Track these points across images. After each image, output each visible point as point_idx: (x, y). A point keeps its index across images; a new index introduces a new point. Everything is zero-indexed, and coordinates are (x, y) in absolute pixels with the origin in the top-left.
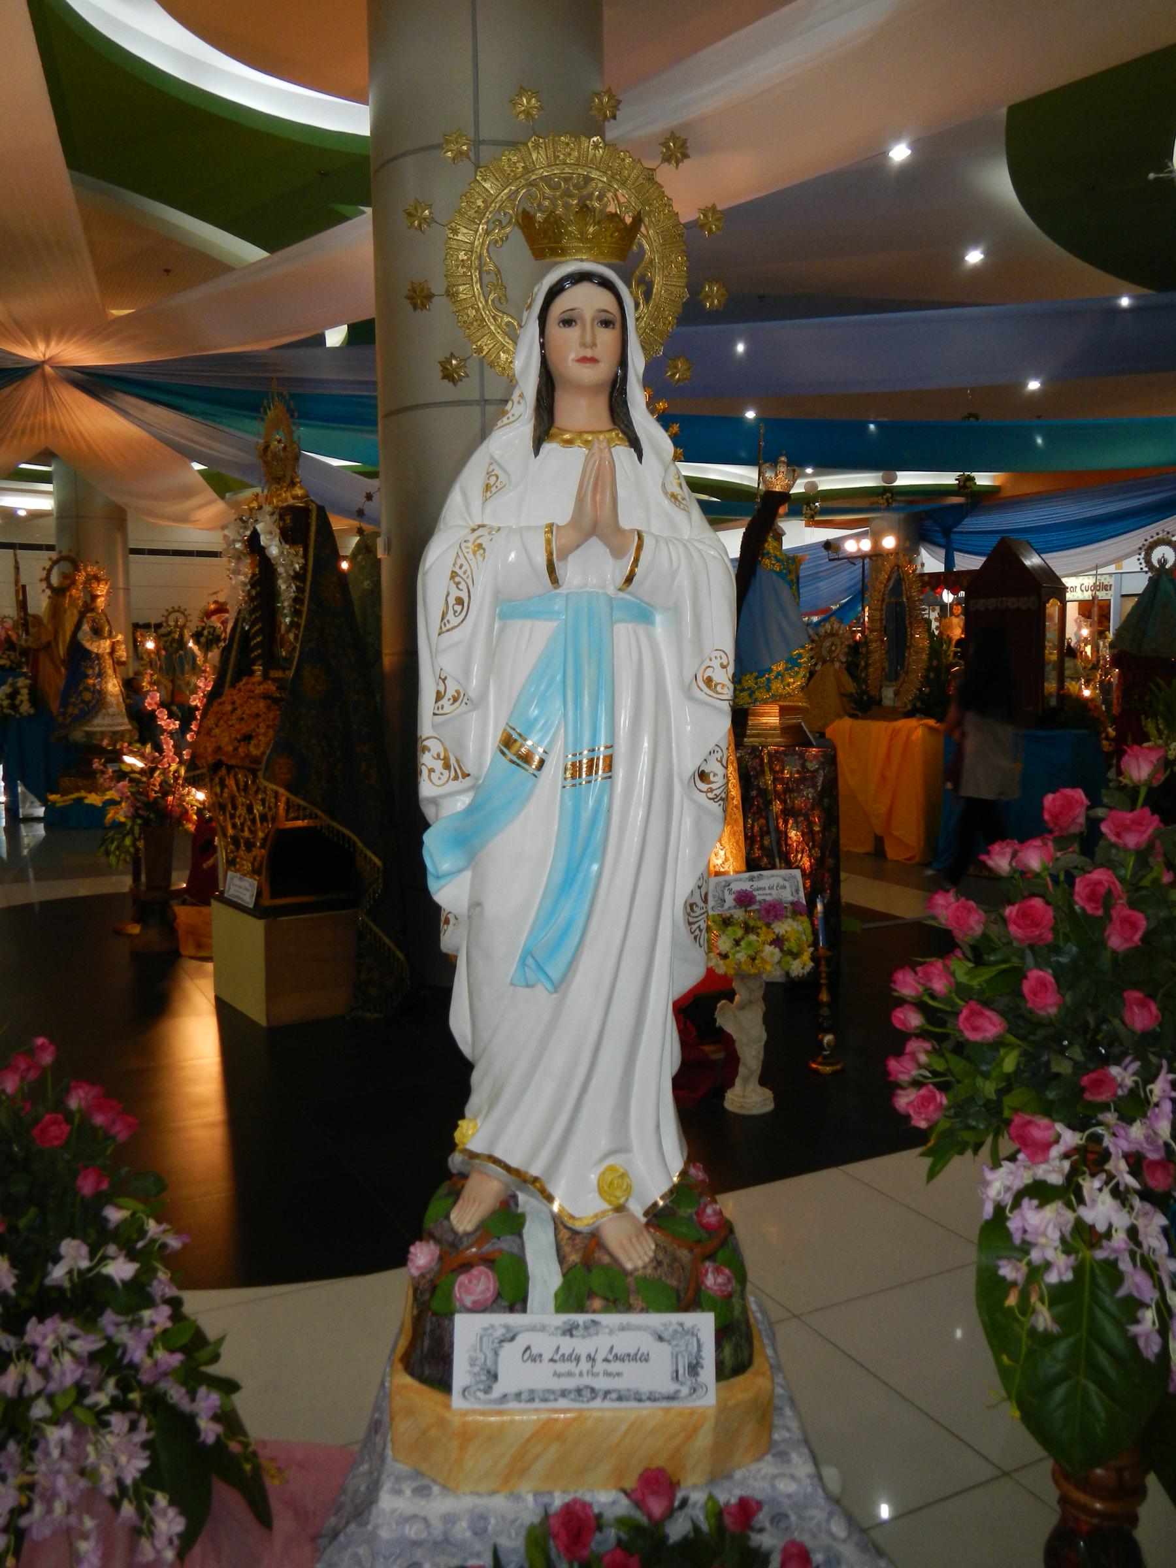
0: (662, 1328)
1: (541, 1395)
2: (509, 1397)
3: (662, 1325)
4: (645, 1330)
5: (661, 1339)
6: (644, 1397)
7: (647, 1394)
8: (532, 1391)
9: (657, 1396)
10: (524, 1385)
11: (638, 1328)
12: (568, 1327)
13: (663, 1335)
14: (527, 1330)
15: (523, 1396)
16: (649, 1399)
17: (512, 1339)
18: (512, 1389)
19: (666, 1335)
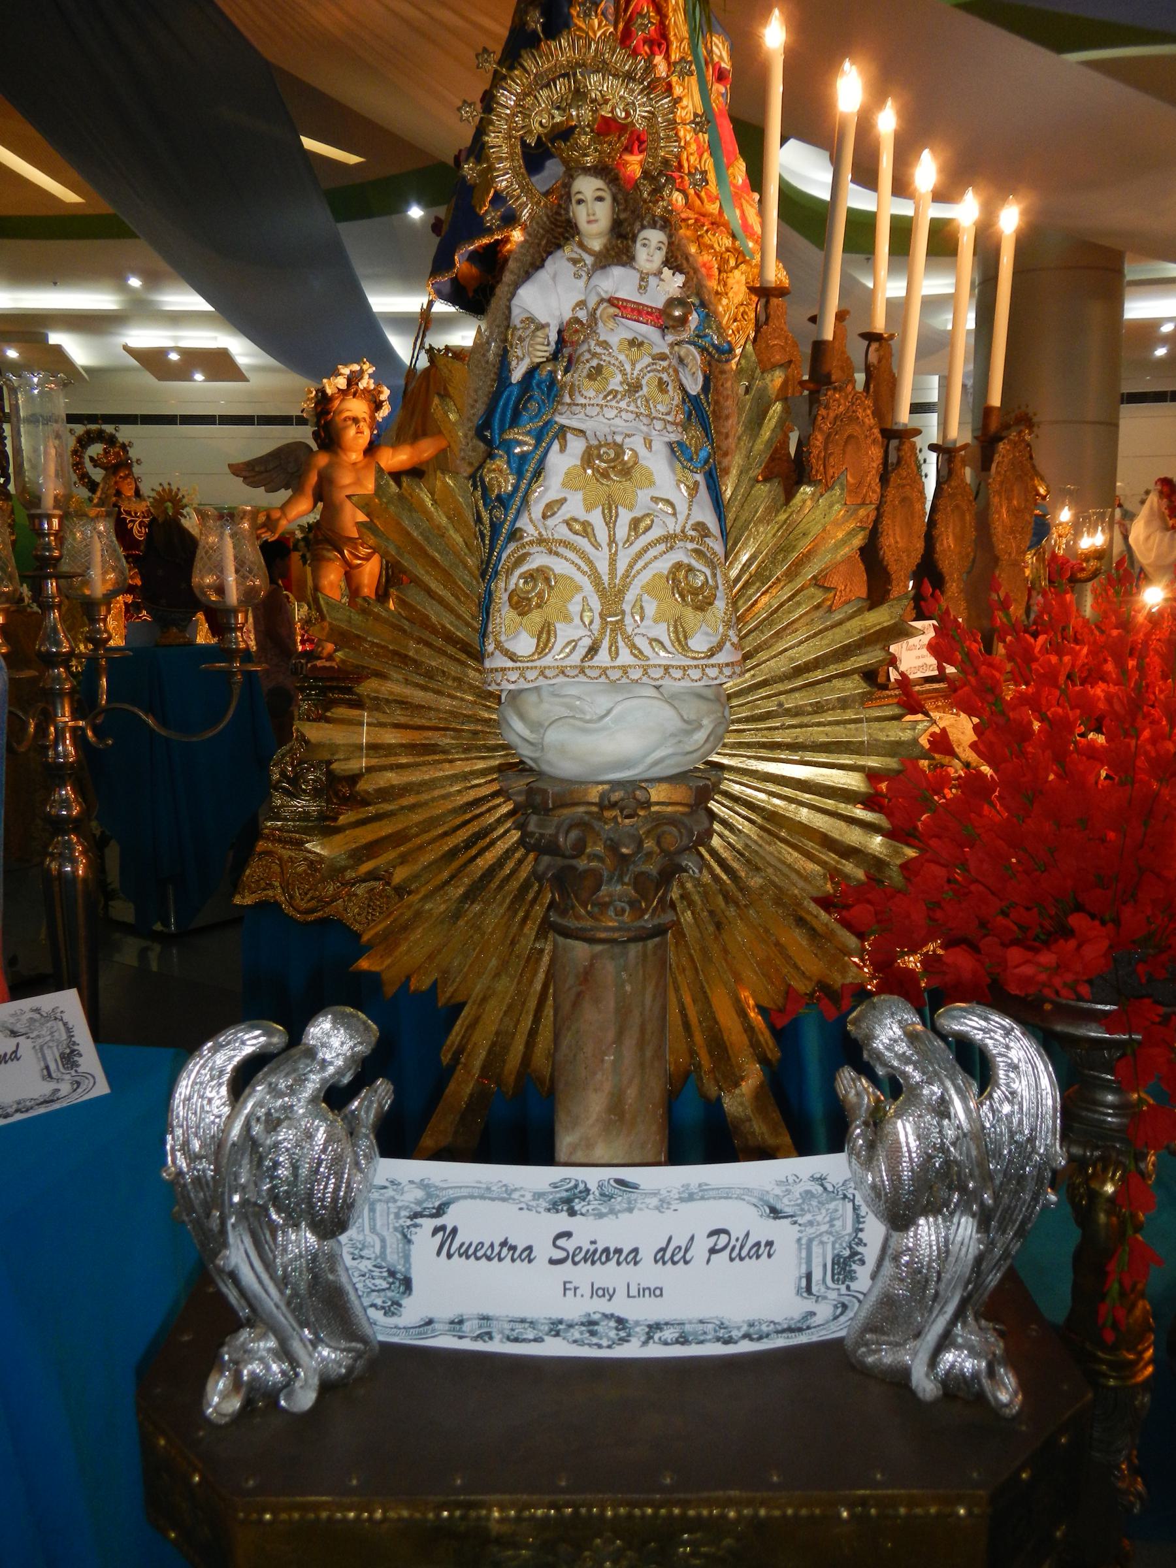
0: (778, 1191)
1: (507, 1326)
2: (436, 1326)
3: (779, 1183)
4: (739, 1198)
5: (775, 1213)
6: (736, 1334)
7: (745, 1329)
8: (486, 1318)
9: (764, 1328)
10: (470, 1308)
11: (725, 1194)
12: (564, 1194)
13: (779, 1207)
14: (472, 1197)
15: (467, 1327)
16: (747, 1336)
17: (440, 1211)
18: (444, 1312)
19: (785, 1206)
